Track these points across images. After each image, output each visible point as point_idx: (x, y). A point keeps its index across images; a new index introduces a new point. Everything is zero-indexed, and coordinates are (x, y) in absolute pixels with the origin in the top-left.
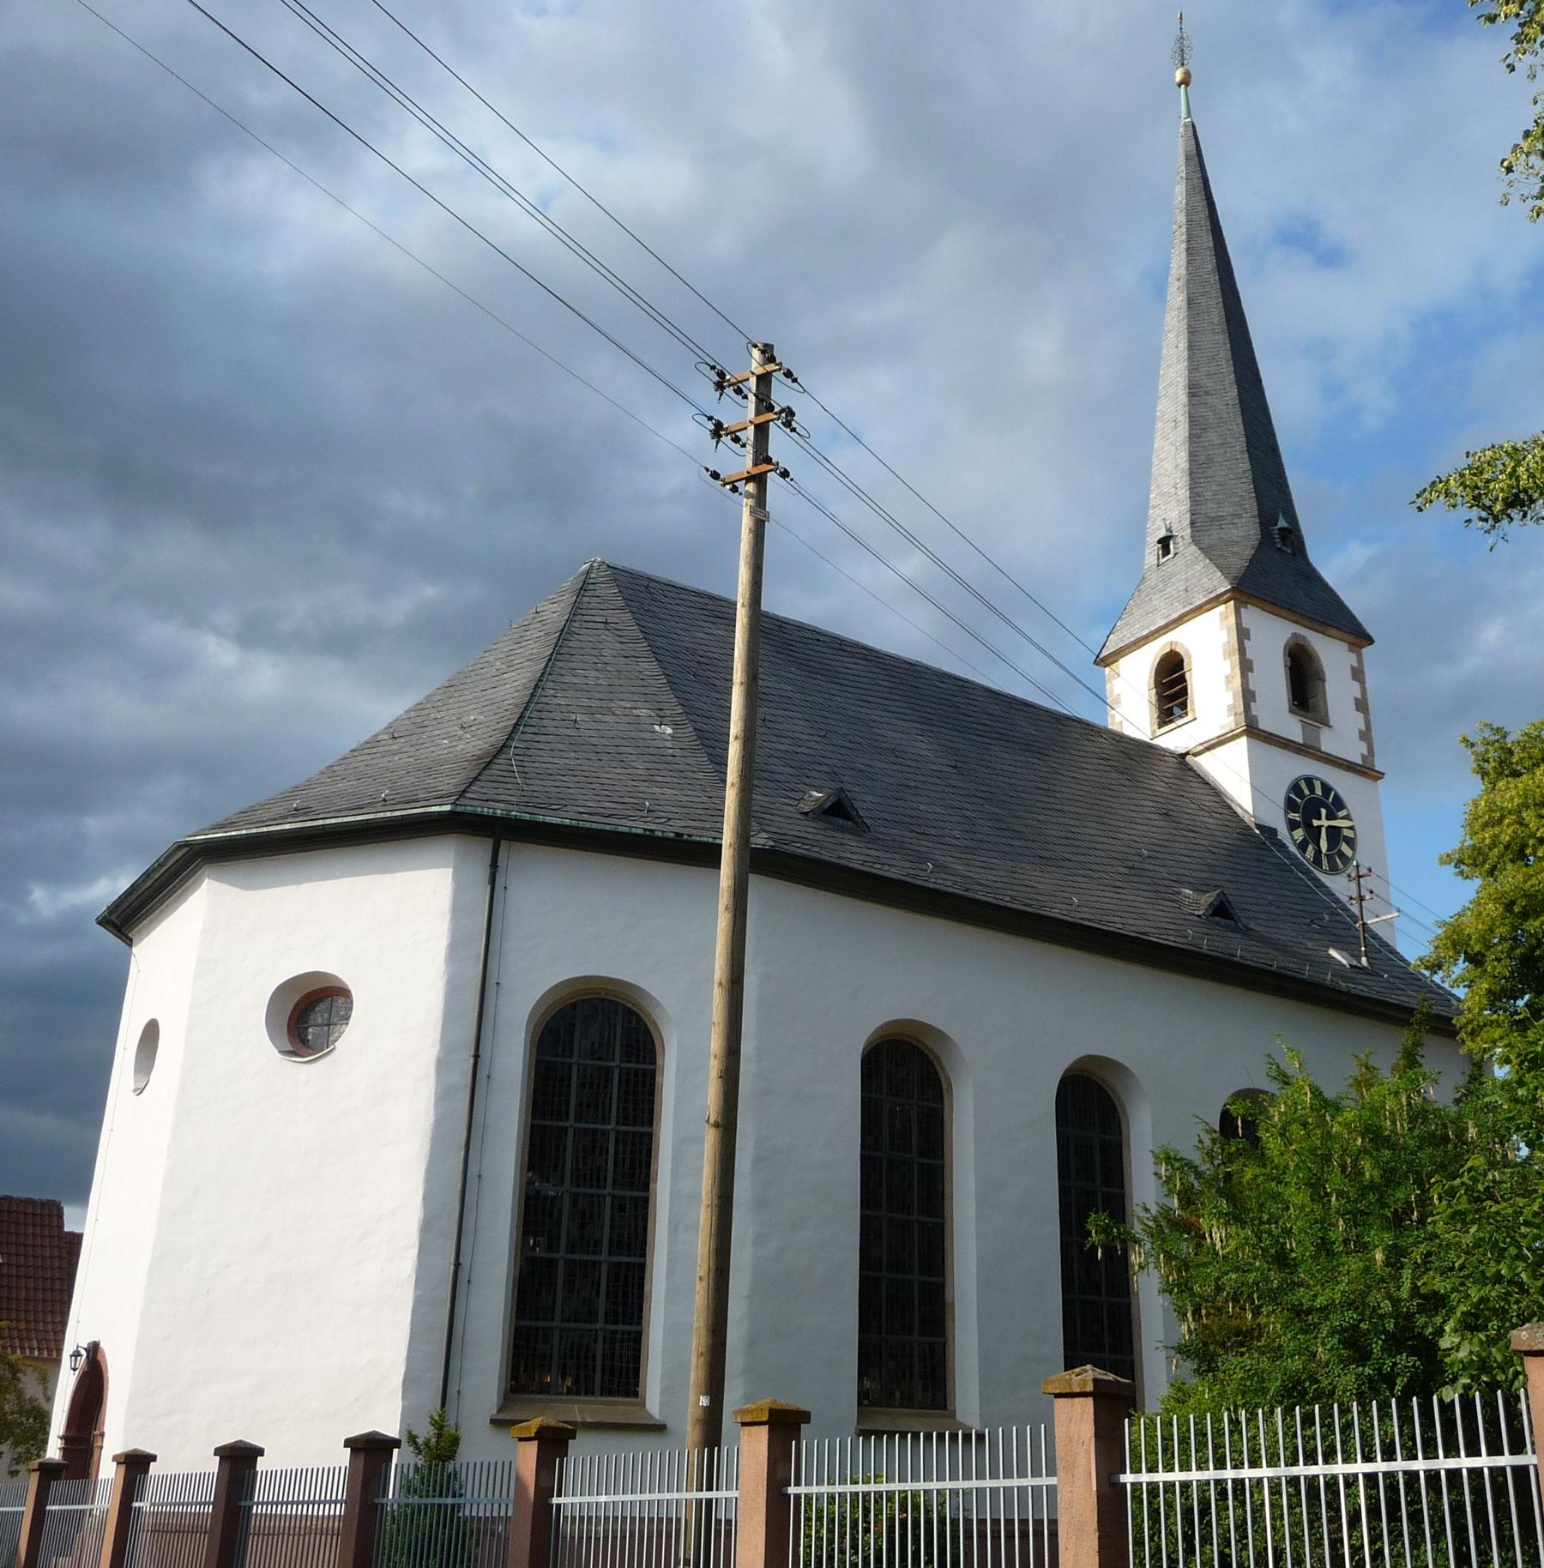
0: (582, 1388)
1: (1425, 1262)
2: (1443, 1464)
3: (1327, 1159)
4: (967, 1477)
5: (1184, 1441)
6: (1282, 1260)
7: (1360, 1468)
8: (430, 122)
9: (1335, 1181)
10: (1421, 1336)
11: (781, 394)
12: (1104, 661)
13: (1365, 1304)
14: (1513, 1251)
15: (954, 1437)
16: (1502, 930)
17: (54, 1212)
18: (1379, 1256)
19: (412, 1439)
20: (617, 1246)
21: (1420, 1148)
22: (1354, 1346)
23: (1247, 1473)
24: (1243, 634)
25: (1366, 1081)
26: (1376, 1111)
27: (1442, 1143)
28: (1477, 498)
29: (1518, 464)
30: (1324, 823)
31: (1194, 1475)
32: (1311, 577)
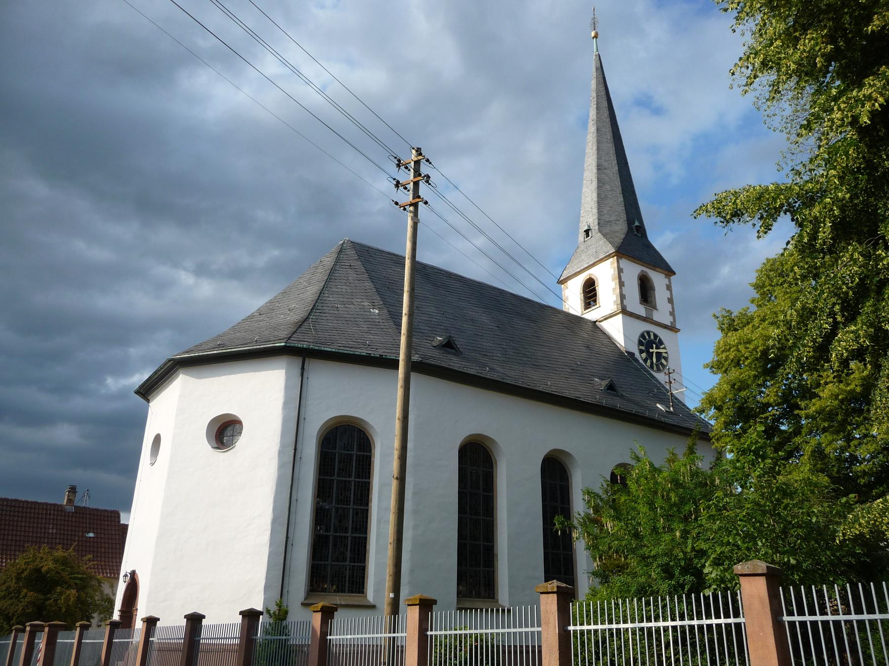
0: (340, 590)
1: (697, 536)
2: (705, 622)
3: (656, 493)
4: (503, 627)
5: (595, 612)
6: (637, 536)
7: (670, 623)
8: (276, 54)
9: (659, 502)
10: (696, 567)
11: (424, 169)
12: (561, 282)
13: (672, 555)
14: (735, 532)
15: (498, 611)
16: (730, 396)
17: (116, 515)
18: (678, 534)
19: (268, 611)
20: (355, 530)
21: (695, 488)
22: (667, 572)
23: (622, 626)
24: (620, 270)
25: (672, 461)
26: (677, 472)
27: (704, 486)
28: (719, 213)
29: (737, 198)
30: (655, 350)
31: (600, 627)
32: (649, 247)
